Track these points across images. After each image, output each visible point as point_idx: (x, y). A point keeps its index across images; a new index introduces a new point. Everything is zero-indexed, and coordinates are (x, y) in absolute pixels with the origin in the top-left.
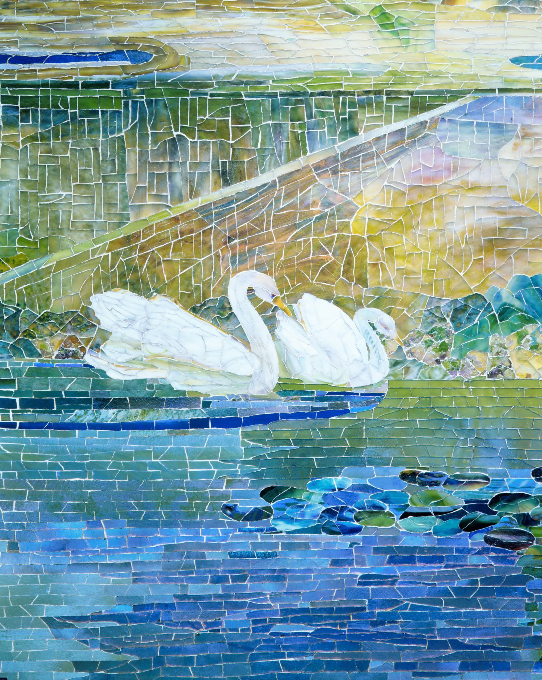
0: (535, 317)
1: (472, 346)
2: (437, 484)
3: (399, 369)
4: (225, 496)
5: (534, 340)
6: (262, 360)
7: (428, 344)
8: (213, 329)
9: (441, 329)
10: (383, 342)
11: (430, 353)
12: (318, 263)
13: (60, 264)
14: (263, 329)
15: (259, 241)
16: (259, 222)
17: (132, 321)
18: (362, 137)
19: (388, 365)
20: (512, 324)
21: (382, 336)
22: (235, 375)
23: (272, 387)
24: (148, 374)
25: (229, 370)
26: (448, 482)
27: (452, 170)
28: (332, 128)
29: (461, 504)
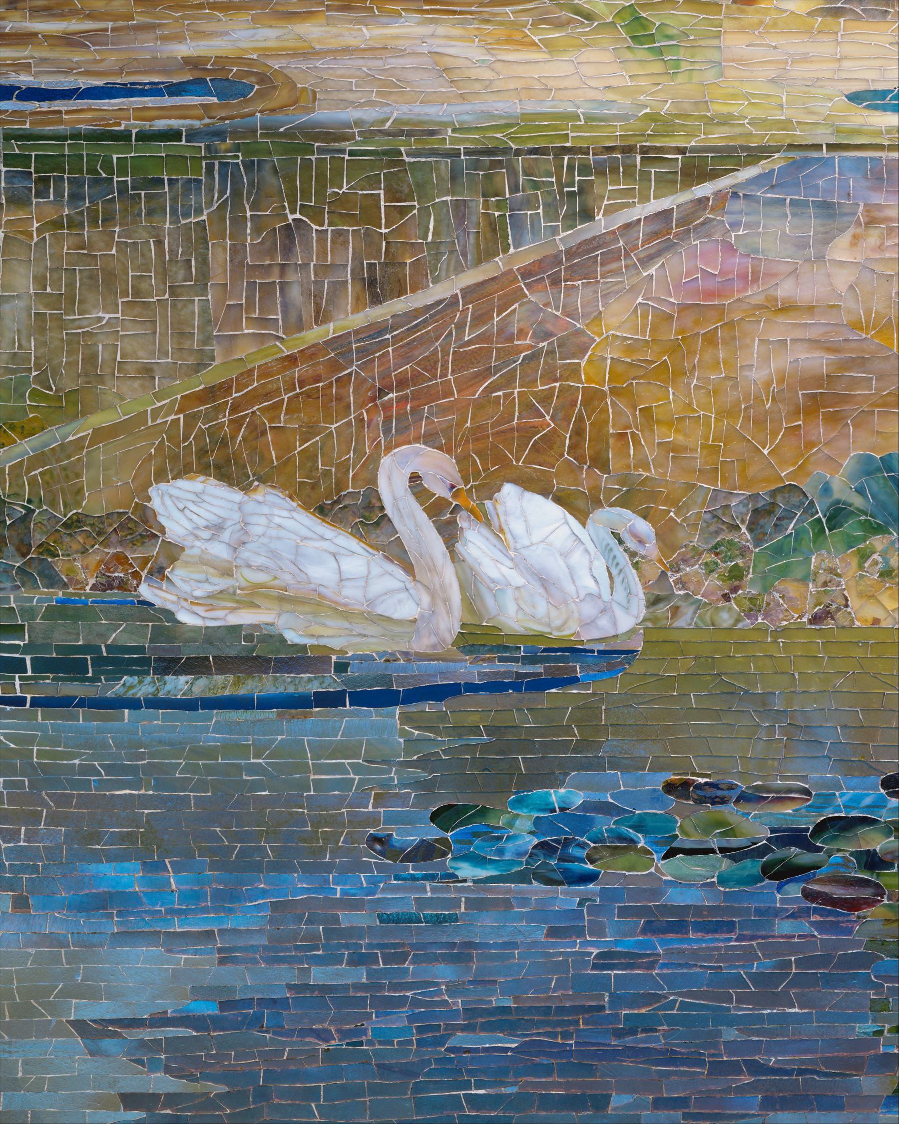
1: (784, 572)
2: (723, 801)
3: (663, 609)
4: (373, 820)
5: (886, 561)
6: (433, 595)
7: (710, 569)
8: (353, 544)
9: (731, 542)
10: (636, 566)
11: (713, 582)
12: (527, 432)
13: (99, 435)
14: (436, 544)
15: (431, 396)
16: (430, 364)
17: (217, 528)
18: (602, 224)
21: (632, 554)
22: (389, 619)
23: (450, 640)
24: (245, 618)
25: (380, 610)
26: (743, 798)
27: (750, 278)
28: (551, 211)
29: (763, 834)
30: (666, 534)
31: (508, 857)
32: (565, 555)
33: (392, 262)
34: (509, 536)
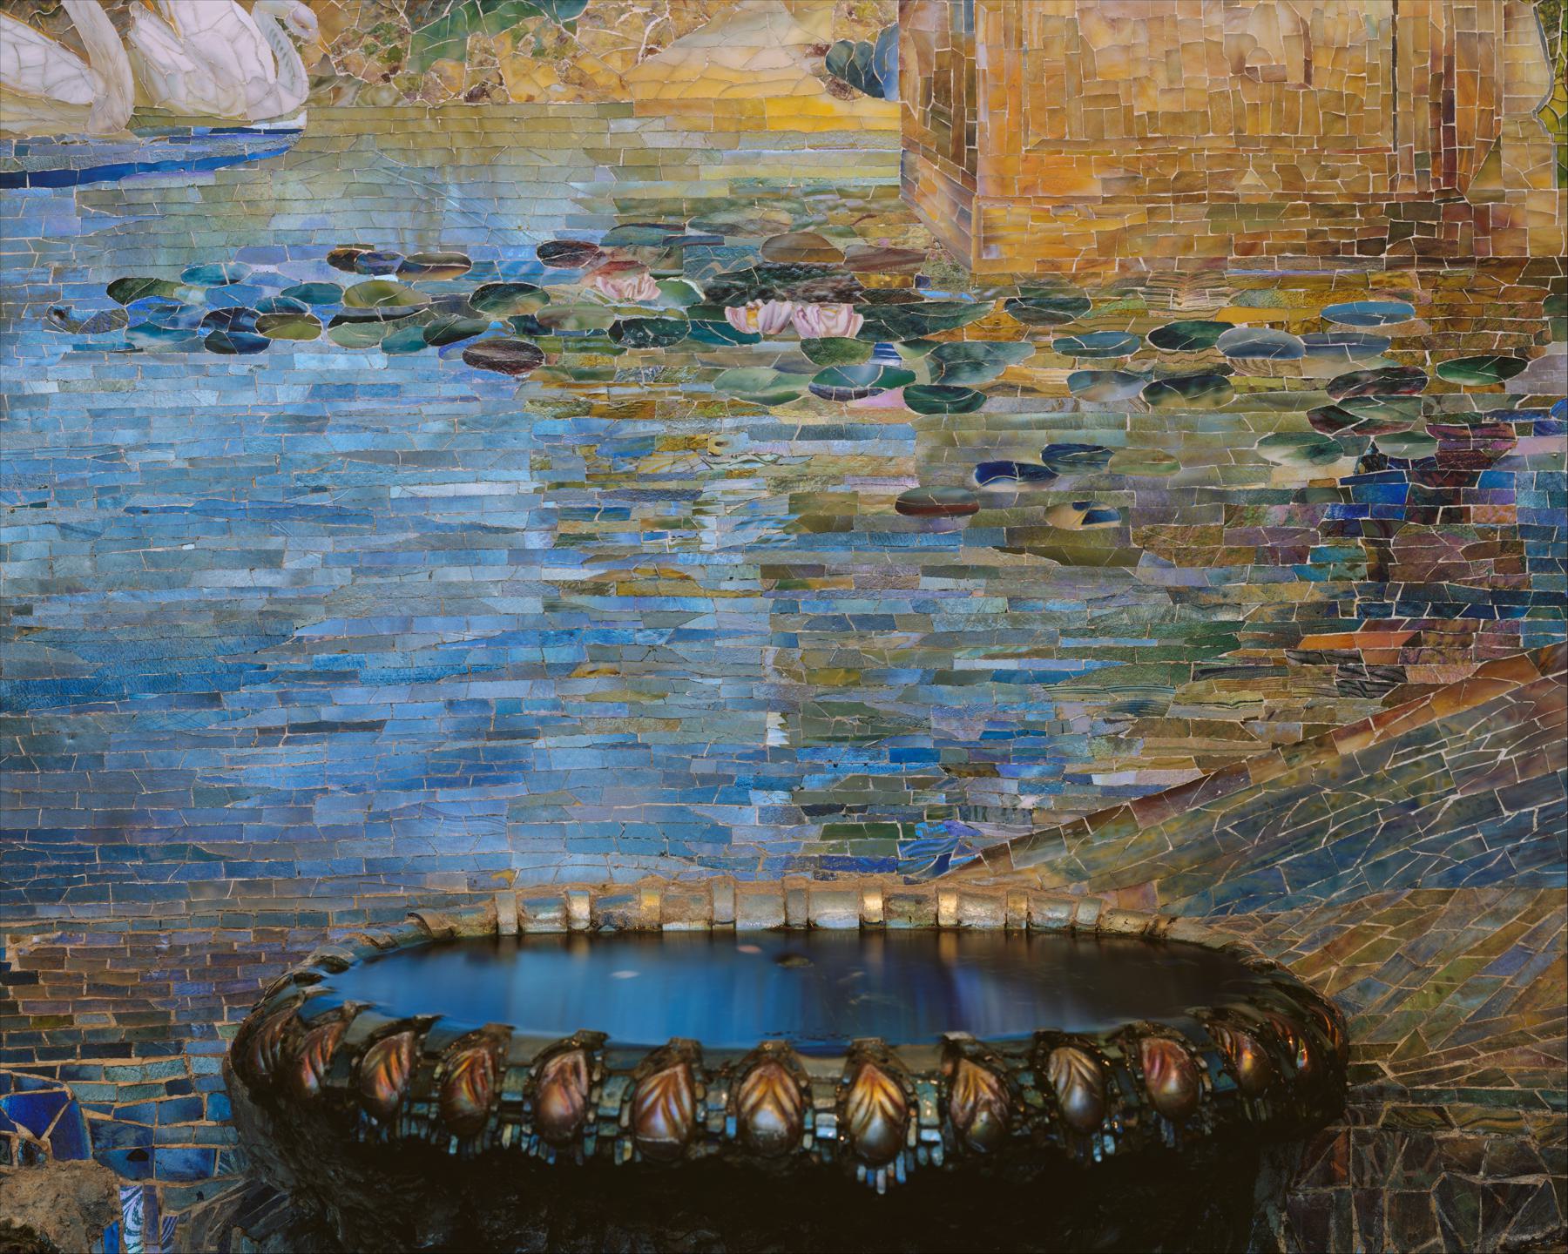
0: (540, 5)
1: (441, 53)
2: (386, 271)
3: (325, 89)
4: (55, 295)
5: (539, 41)
6: (107, 81)
7: (370, 51)
8: (30, 33)
9: (389, 27)
10: (299, 49)
11: (376, 65)
14: (109, 33)
19: (307, 85)
20: (502, 18)
21: (296, 39)
22: (65, 104)
23: (123, 123)
25: (57, 96)
26: (405, 269)
31: (181, 327)
32: (232, 41)
34: (178, 24)
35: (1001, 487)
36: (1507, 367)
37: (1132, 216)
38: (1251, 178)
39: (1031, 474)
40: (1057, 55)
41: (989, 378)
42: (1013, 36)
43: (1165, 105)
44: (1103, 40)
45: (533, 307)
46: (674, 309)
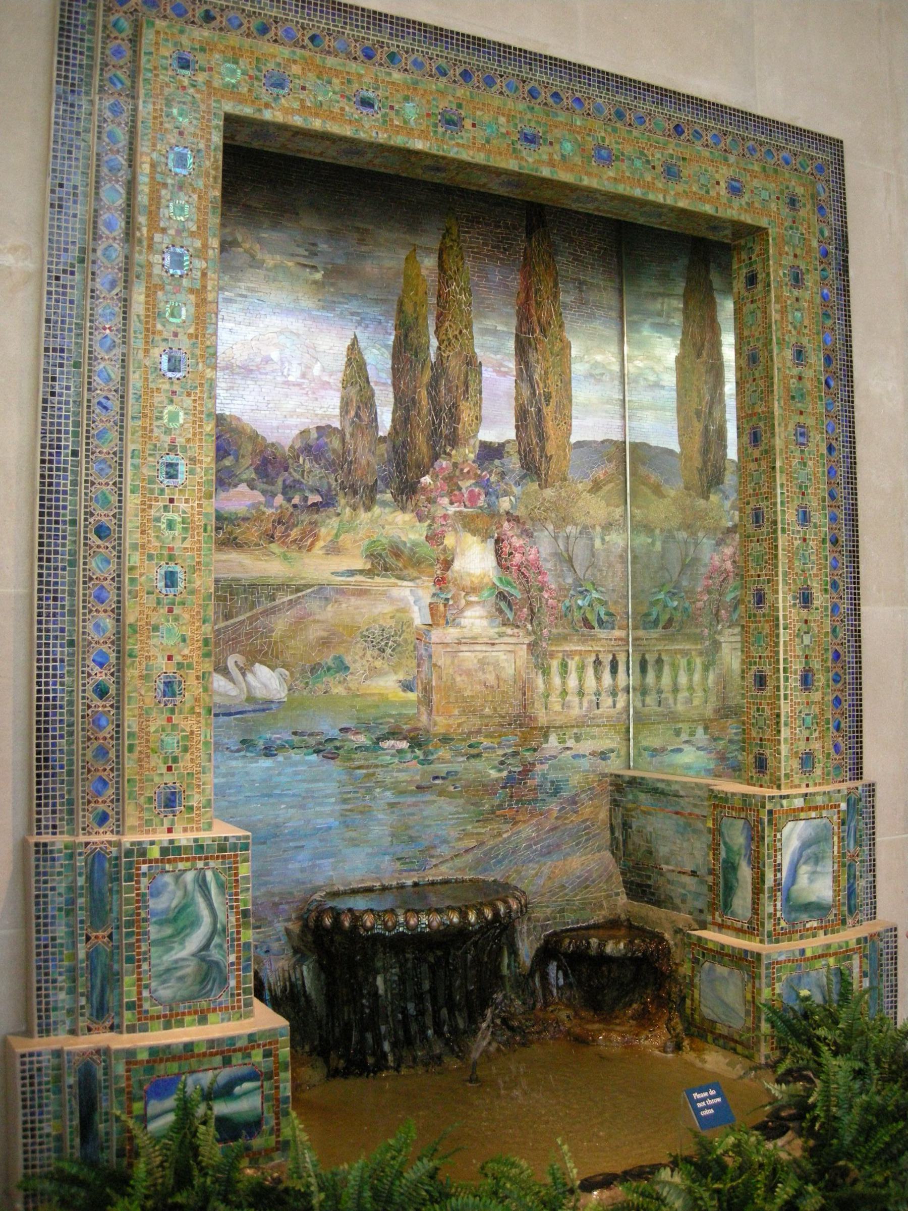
11: (303, 685)
12: (261, 651)
14: (241, 678)
18: (277, 602)
27: (310, 615)
29: (313, 743)
30: (292, 674)
33: (231, 611)
35: (437, 782)
36: (535, 750)
37: (463, 719)
38: (487, 710)
39: (443, 778)
40: (449, 683)
41: (435, 757)
42: (440, 678)
43: (470, 694)
44: (458, 679)
45: (338, 744)
46: (368, 743)
